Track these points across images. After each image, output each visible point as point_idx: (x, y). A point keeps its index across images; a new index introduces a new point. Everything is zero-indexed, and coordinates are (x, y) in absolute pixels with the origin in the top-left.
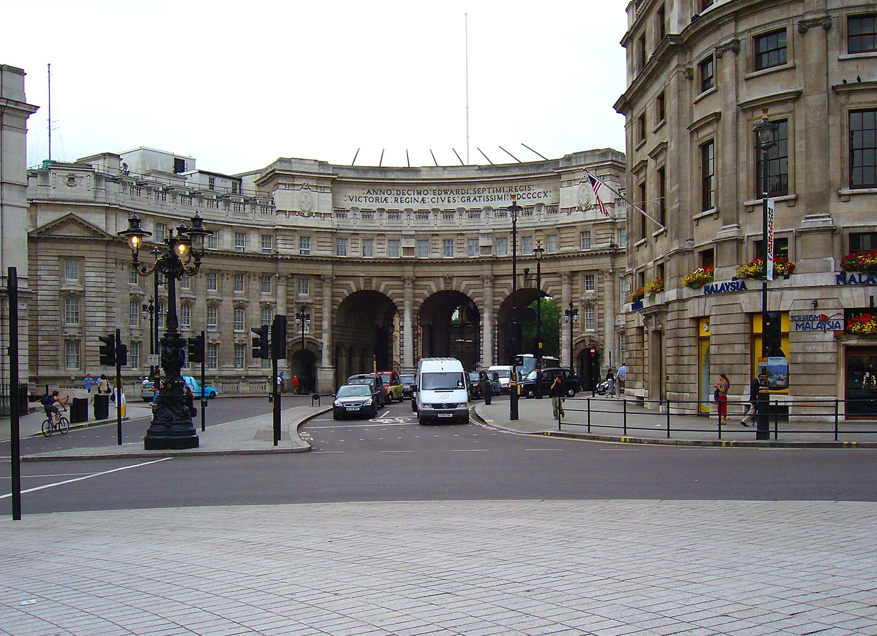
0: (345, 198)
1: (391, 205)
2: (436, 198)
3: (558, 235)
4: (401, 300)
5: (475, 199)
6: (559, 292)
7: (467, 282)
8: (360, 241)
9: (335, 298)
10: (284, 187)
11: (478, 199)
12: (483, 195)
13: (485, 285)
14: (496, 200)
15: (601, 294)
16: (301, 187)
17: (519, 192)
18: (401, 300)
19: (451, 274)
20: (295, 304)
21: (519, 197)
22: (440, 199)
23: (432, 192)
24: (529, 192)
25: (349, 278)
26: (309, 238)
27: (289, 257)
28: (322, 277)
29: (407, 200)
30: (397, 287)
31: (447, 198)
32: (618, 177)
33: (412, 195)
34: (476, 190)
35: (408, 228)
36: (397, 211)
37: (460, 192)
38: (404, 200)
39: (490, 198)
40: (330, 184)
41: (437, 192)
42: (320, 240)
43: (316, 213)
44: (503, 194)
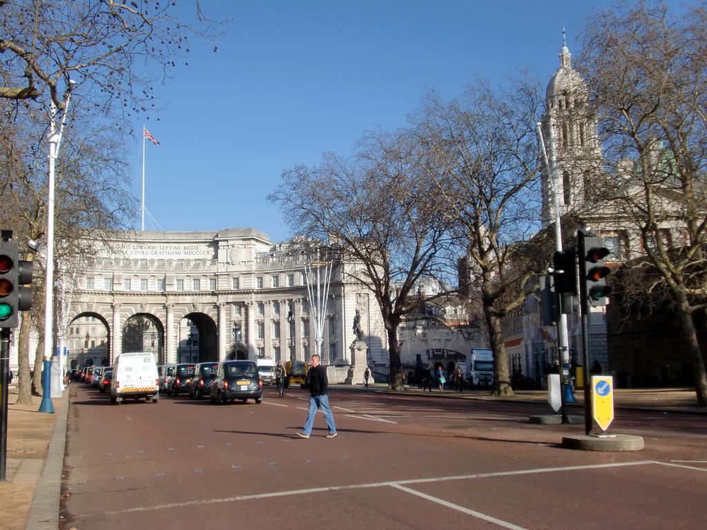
6: (218, 315)
19: (145, 302)
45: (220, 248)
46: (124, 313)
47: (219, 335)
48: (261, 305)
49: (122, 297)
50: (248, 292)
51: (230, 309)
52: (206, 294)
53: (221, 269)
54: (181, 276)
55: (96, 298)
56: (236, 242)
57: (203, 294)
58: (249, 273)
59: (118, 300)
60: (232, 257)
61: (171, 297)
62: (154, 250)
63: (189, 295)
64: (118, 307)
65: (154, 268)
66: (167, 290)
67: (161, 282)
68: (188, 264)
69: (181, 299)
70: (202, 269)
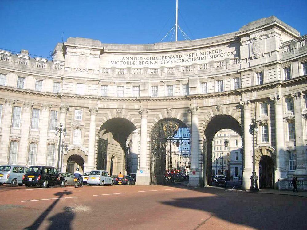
2: (164, 61)
4: (139, 124)
5: (187, 60)
6: (243, 117)
9: (97, 123)
10: (70, 54)
11: (189, 60)
14: (200, 59)
16: (80, 54)
17: (215, 54)
18: (139, 124)
19: (171, 107)
21: (215, 56)
22: (166, 62)
24: (222, 53)
29: (146, 63)
31: (170, 61)
32: (280, 35)
34: (189, 55)
35: (145, 79)
36: (138, 69)
37: (178, 57)
38: (144, 63)
41: (164, 57)
42: (90, 85)
43: (89, 69)
44: (205, 55)
45: (242, 44)
46: (152, 118)
48: (289, 99)
49: (149, 103)
50: (273, 86)
51: (255, 108)
52: (229, 94)
54: (205, 79)
55: (124, 105)
56: (257, 34)
57: (226, 95)
58: (273, 64)
59: (144, 105)
60: (254, 51)
62: (182, 58)
63: (212, 96)
64: (145, 112)
65: (179, 74)
66: (190, 93)
67: (185, 87)
68: (211, 66)
70: (225, 70)
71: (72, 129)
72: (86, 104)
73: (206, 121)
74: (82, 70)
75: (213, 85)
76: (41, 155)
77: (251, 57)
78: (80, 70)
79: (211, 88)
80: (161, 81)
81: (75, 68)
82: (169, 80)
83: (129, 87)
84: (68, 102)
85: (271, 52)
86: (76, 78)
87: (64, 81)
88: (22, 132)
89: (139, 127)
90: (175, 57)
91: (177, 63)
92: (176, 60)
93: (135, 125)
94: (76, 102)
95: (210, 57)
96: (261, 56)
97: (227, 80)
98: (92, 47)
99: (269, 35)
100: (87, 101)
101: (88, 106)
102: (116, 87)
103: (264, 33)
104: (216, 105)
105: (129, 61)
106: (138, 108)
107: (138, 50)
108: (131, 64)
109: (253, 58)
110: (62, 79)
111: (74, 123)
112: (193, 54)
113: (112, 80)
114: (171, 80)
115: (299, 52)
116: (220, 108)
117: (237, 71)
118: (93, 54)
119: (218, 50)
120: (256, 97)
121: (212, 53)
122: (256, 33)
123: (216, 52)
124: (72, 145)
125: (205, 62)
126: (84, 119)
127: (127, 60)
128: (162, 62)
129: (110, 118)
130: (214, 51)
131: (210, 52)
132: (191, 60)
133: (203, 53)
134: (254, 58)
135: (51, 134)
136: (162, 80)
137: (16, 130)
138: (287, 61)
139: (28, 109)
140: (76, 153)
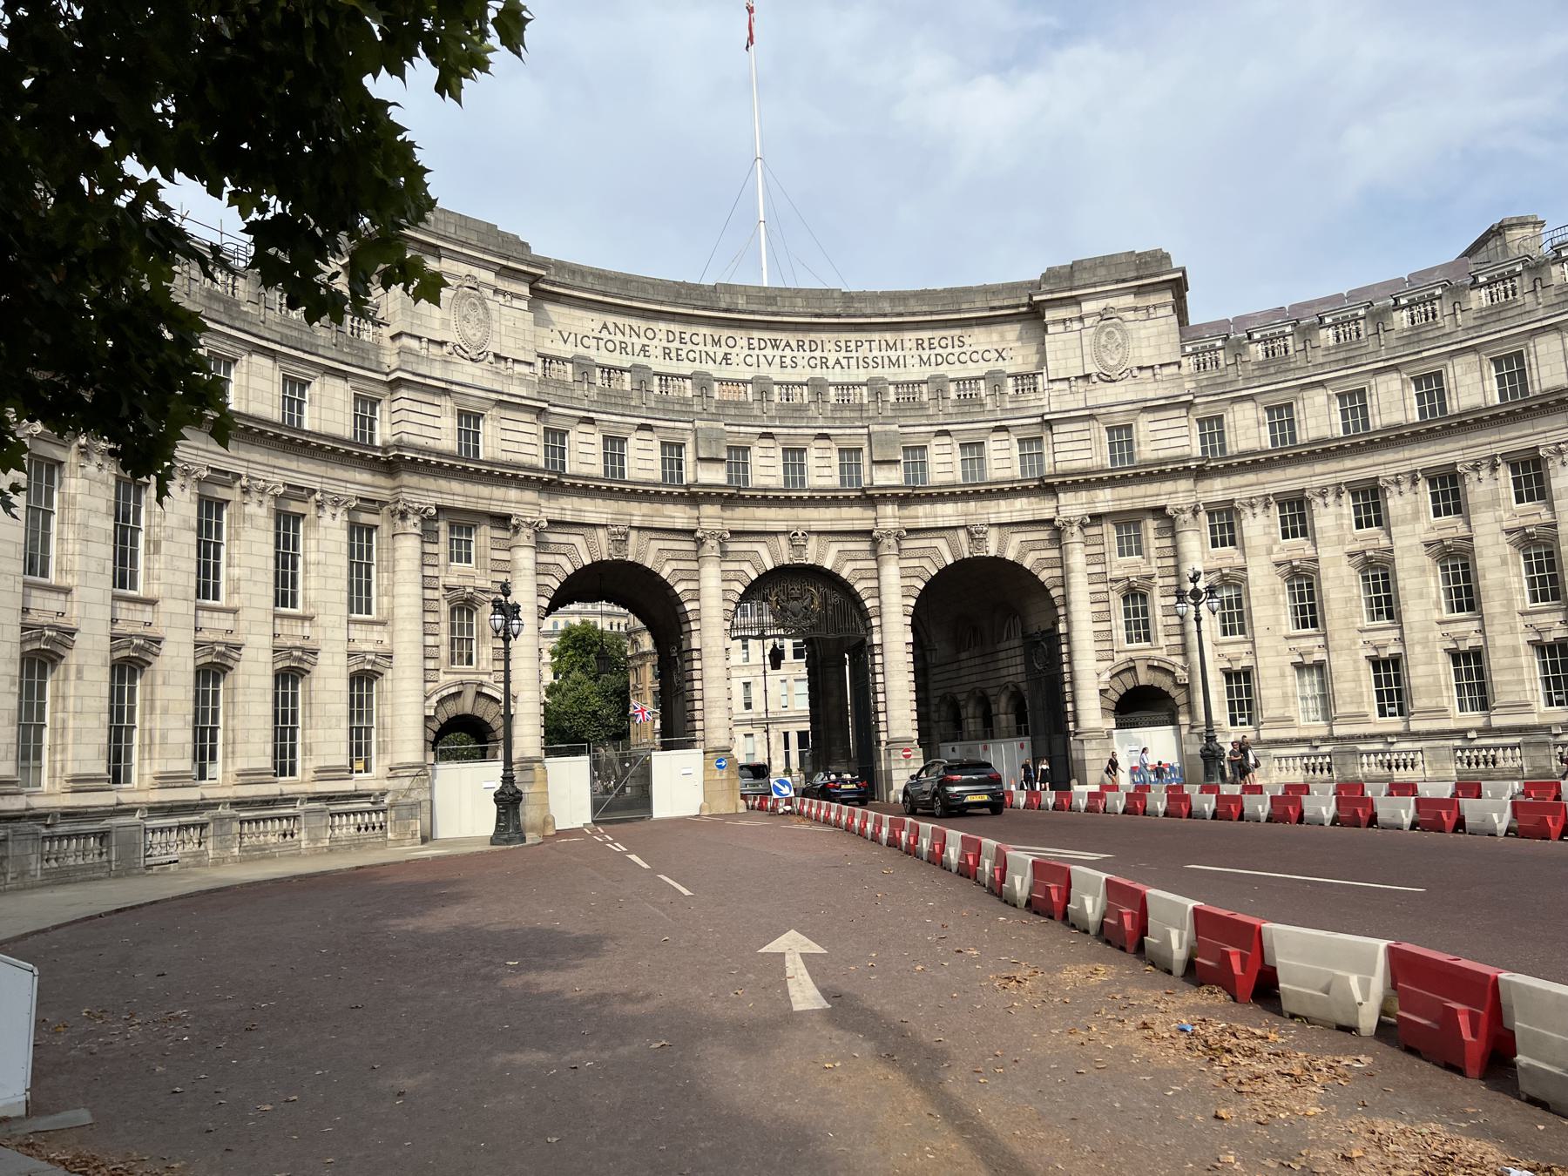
0: (552, 335)
1: (658, 364)
2: (755, 357)
3: (1047, 438)
4: (692, 585)
5: (838, 362)
7: (840, 546)
8: (598, 439)
11: (845, 363)
12: (854, 354)
13: (883, 550)
14: (886, 366)
15: (1171, 562)
18: (692, 585)
19: (805, 526)
20: (442, 591)
21: (940, 359)
22: (762, 359)
23: (744, 343)
24: (964, 349)
25: (574, 530)
26: (478, 417)
27: (434, 460)
28: (513, 521)
29: (691, 355)
30: (681, 555)
31: (777, 360)
33: (701, 347)
34: (843, 344)
35: (705, 416)
37: (806, 347)
38: (683, 353)
39: (871, 363)
40: (528, 290)
41: (755, 343)
43: (496, 356)
44: (899, 352)
45: (1050, 329)
47: (1068, 634)
53: (1055, 400)
55: (639, 512)
56: (1112, 302)
59: (711, 517)
61: (889, 510)
62: (818, 354)
69: (924, 514)
71: (444, 607)
72: (500, 503)
73: (927, 578)
74: (473, 354)
75: (948, 458)
76: (330, 728)
77: (1087, 377)
78: (466, 355)
79: (941, 468)
80: (765, 430)
81: (442, 344)
82: (792, 431)
83: (649, 445)
84: (427, 490)
85: (1161, 366)
86: (455, 388)
87: (403, 393)
88: (243, 625)
89: (689, 595)
90: (794, 344)
91: (803, 371)
92: (799, 358)
93: (678, 589)
94: (459, 494)
95: (921, 359)
96: (1124, 375)
97: (998, 445)
98: (504, 262)
99: (1151, 310)
100: (499, 492)
101: (506, 510)
102: (599, 438)
103: (1129, 300)
104: (962, 523)
105: (627, 339)
106: (686, 527)
107: (662, 303)
108: (636, 352)
109: (1095, 379)
110: (397, 384)
111: (453, 581)
112: (859, 344)
113: (589, 411)
114: (799, 431)
115: (1256, 373)
116: (981, 536)
117: (1042, 416)
118: (504, 293)
119: (950, 339)
120: (1110, 503)
121: (926, 345)
122: (1107, 297)
123: (944, 345)
124: (449, 677)
125: (902, 379)
126: (489, 564)
127: (619, 337)
128: (748, 359)
129: (646, 565)
130: (936, 342)
131: (920, 342)
132: (853, 362)
133: (895, 343)
134: (1103, 380)
135: (358, 626)
136: (767, 427)
137: (216, 615)
138: (1216, 398)
139: (263, 511)
140: (467, 705)
